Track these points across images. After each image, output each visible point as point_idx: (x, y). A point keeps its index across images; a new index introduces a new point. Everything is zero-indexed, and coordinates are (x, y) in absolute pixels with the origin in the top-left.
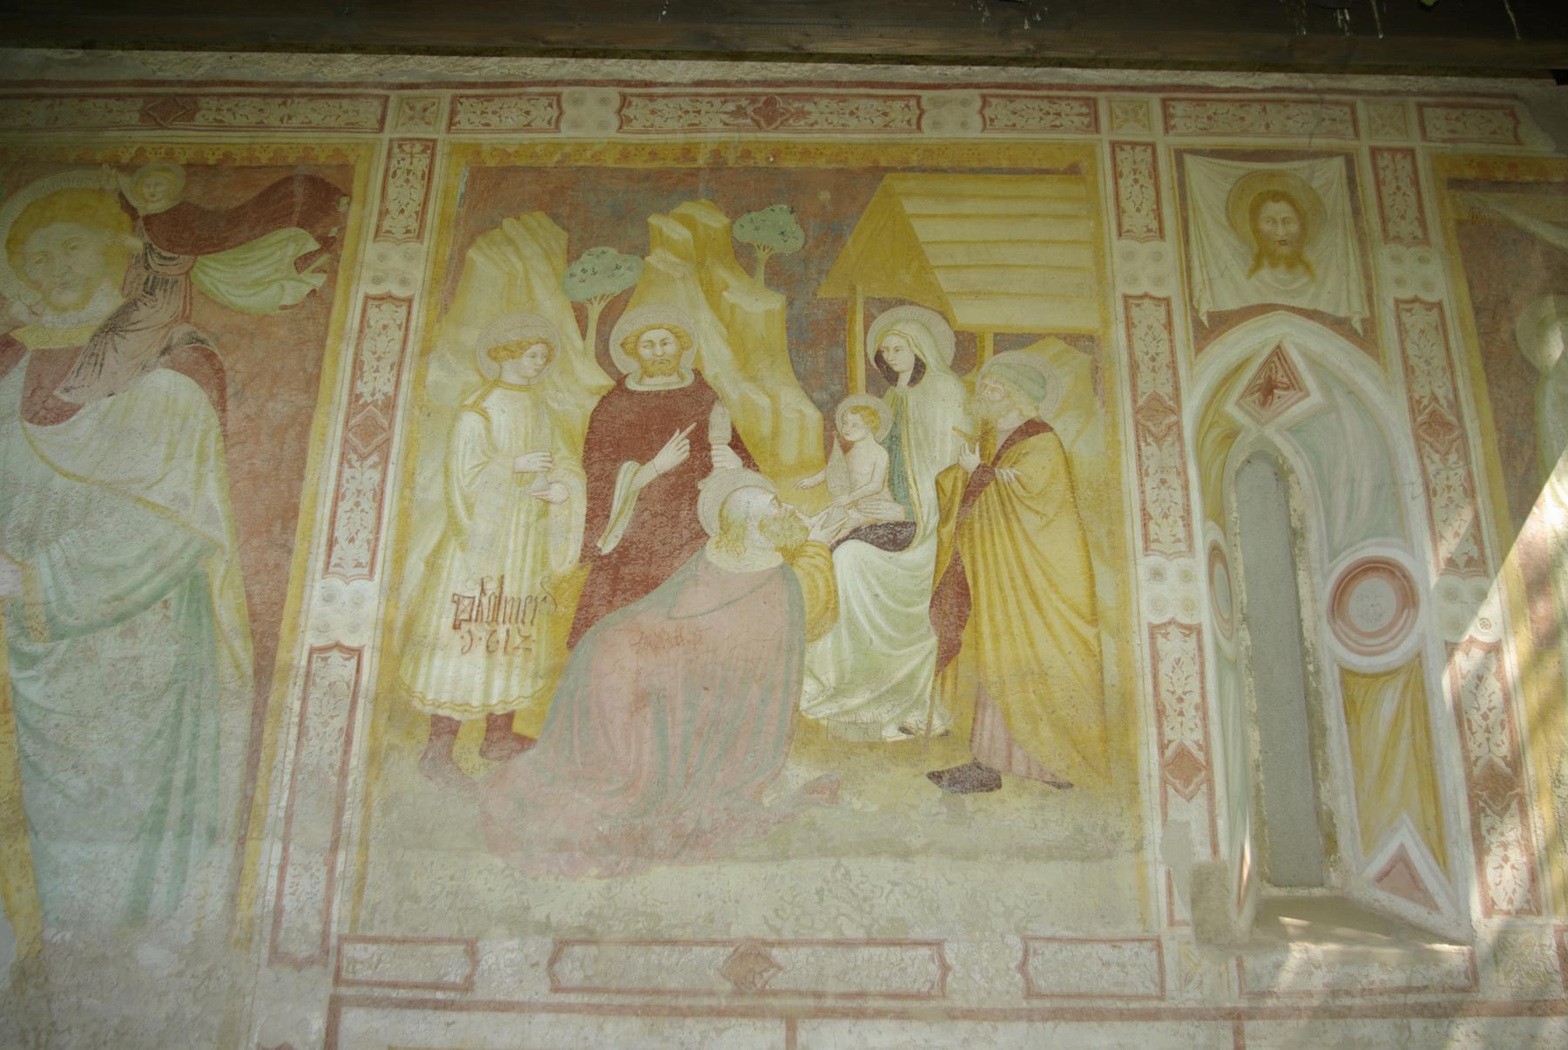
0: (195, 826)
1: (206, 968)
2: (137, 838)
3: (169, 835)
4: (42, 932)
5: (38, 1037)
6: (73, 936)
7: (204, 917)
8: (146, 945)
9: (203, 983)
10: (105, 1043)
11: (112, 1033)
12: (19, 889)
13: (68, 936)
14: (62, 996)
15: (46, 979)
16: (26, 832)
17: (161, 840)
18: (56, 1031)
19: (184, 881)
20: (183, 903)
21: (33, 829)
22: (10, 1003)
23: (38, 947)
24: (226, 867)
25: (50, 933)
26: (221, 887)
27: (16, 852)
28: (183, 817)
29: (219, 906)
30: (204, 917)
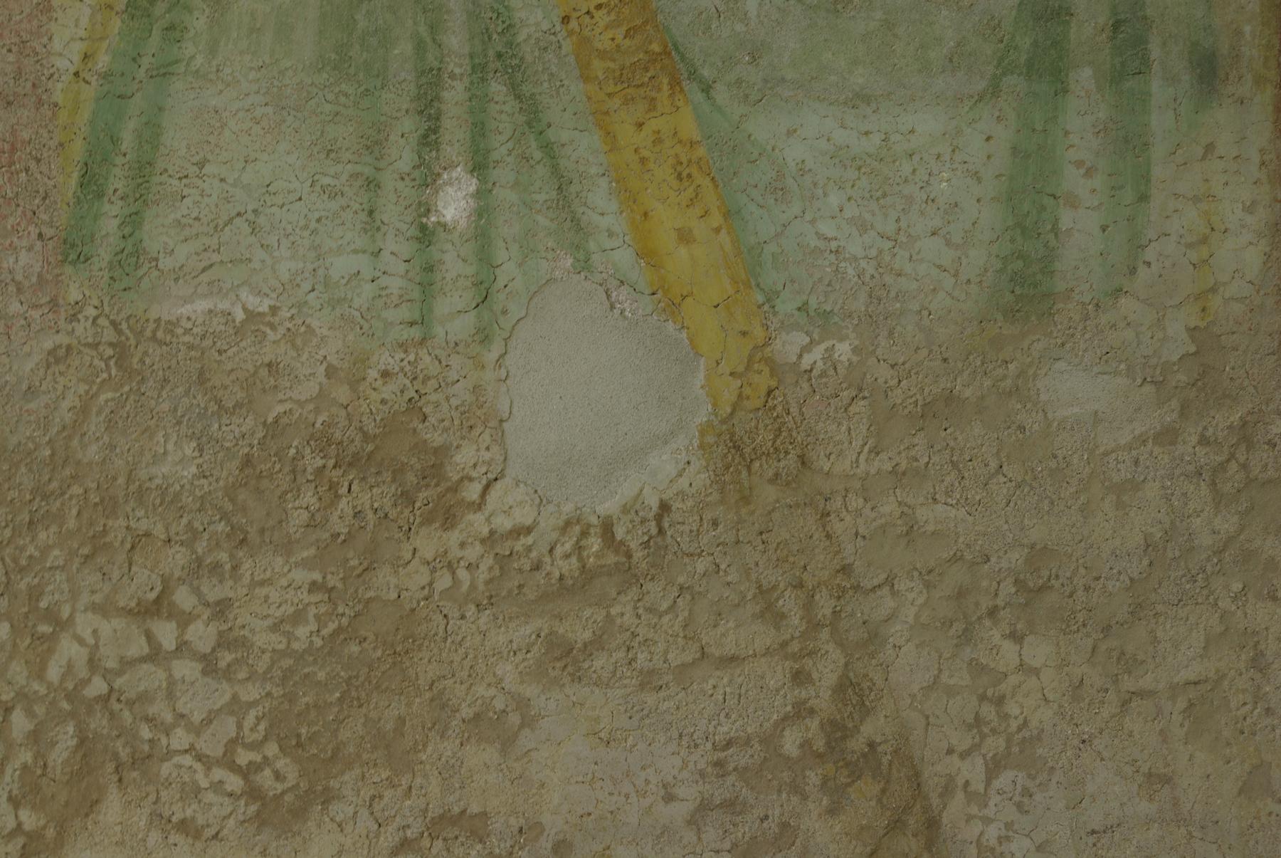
0: (1155, 52)
1: (1235, 418)
2: (994, 90)
3: (1083, 78)
4: (769, 341)
5: (809, 605)
6: (856, 350)
7: (1213, 290)
8: (1061, 365)
9: (1232, 456)
10: (993, 612)
11: (1008, 588)
12: (685, 237)
13: (843, 350)
14: (856, 502)
15: (803, 461)
16: (675, 83)
17: (1063, 90)
18: (856, 588)
19: (1143, 198)
20: (1150, 254)
21: (693, 74)
22: (715, 523)
23: (763, 381)
24: (1256, 158)
25: (789, 345)
26: (1250, 209)
27: (658, 141)
28: (1116, 26)
29: (1253, 259)
30: (1213, 290)
